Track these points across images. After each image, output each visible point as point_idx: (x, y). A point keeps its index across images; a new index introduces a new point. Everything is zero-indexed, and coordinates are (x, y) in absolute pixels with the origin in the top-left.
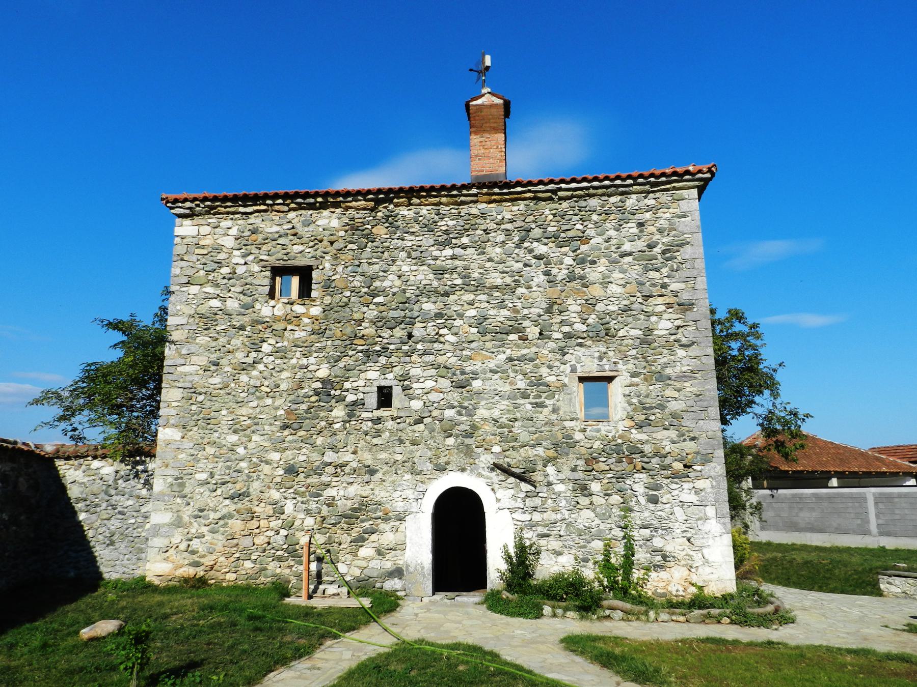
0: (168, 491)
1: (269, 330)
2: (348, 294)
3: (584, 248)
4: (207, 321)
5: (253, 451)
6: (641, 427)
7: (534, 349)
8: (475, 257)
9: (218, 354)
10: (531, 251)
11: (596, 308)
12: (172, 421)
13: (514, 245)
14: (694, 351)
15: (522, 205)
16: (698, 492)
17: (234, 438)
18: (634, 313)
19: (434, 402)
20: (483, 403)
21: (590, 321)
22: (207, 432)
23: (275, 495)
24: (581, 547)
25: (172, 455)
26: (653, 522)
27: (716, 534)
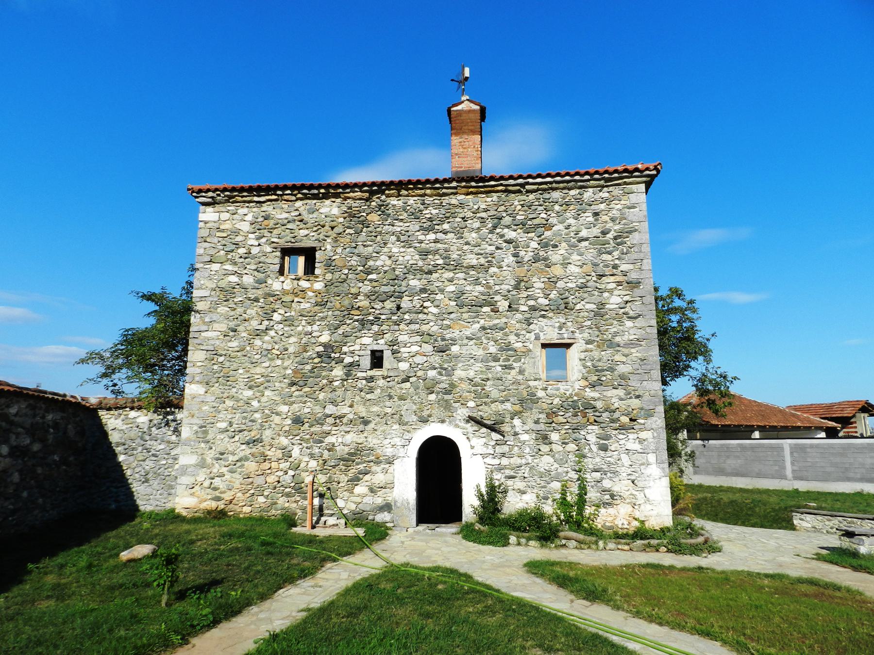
0: (194, 437)
2: (346, 271)
3: (548, 234)
4: (226, 294)
5: (266, 404)
6: (594, 386)
7: (504, 320)
9: (236, 322)
10: (502, 236)
11: (557, 285)
12: (197, 379)
13: (487, 231)
14: (640, 322)
15: (495, 197)
16: (641, 441)
17: (249, 393)
18: (590, 289)
20: (460, 365)
21: (552, 296)
22: (227, 387)
23: (284, 441)
24: (542, 487)
25: (197, 406)
26: (603, 466)
27: (656, 477)
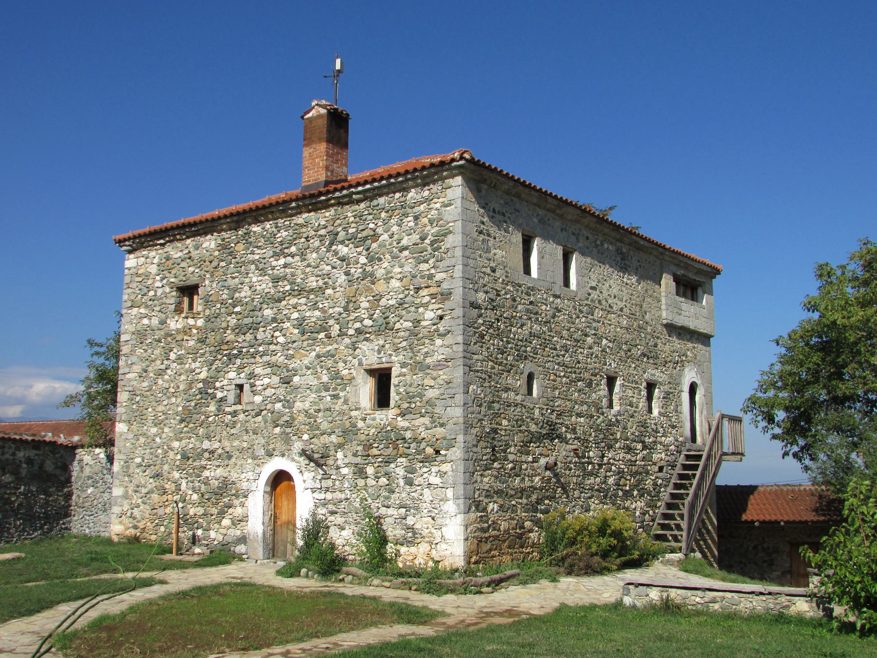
1: (174, 341)
5: (164, 441)
7: (335, 346)
8: (299, 264)
19: (268, 397)
21: (375, 316)
23: (176, 475)
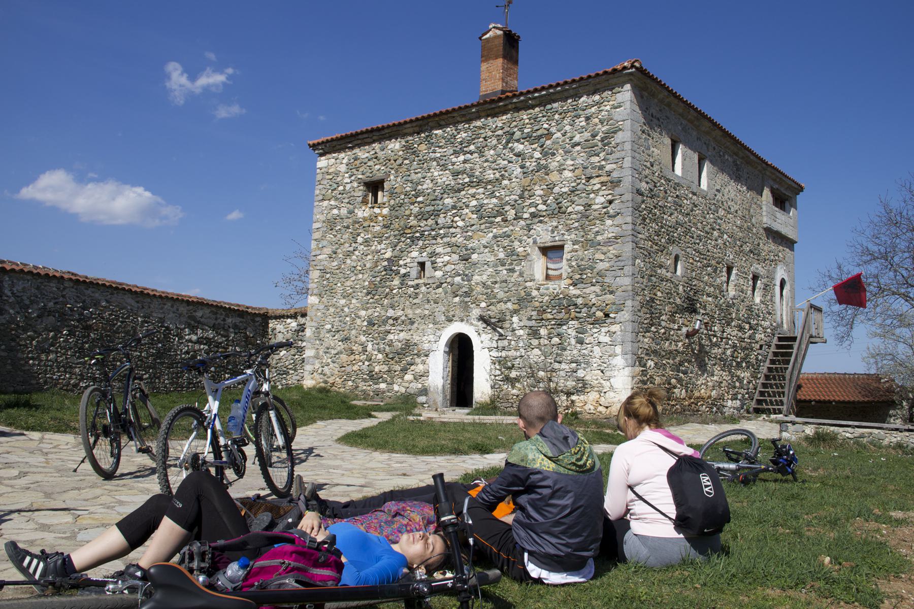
3: (548, 142)
11: (554, 191)
21: (549, 201)
23: (363, 339)
